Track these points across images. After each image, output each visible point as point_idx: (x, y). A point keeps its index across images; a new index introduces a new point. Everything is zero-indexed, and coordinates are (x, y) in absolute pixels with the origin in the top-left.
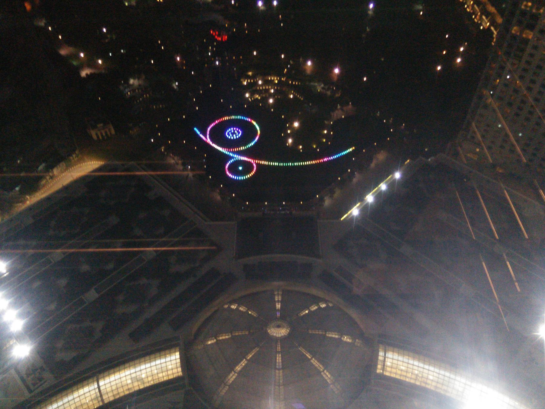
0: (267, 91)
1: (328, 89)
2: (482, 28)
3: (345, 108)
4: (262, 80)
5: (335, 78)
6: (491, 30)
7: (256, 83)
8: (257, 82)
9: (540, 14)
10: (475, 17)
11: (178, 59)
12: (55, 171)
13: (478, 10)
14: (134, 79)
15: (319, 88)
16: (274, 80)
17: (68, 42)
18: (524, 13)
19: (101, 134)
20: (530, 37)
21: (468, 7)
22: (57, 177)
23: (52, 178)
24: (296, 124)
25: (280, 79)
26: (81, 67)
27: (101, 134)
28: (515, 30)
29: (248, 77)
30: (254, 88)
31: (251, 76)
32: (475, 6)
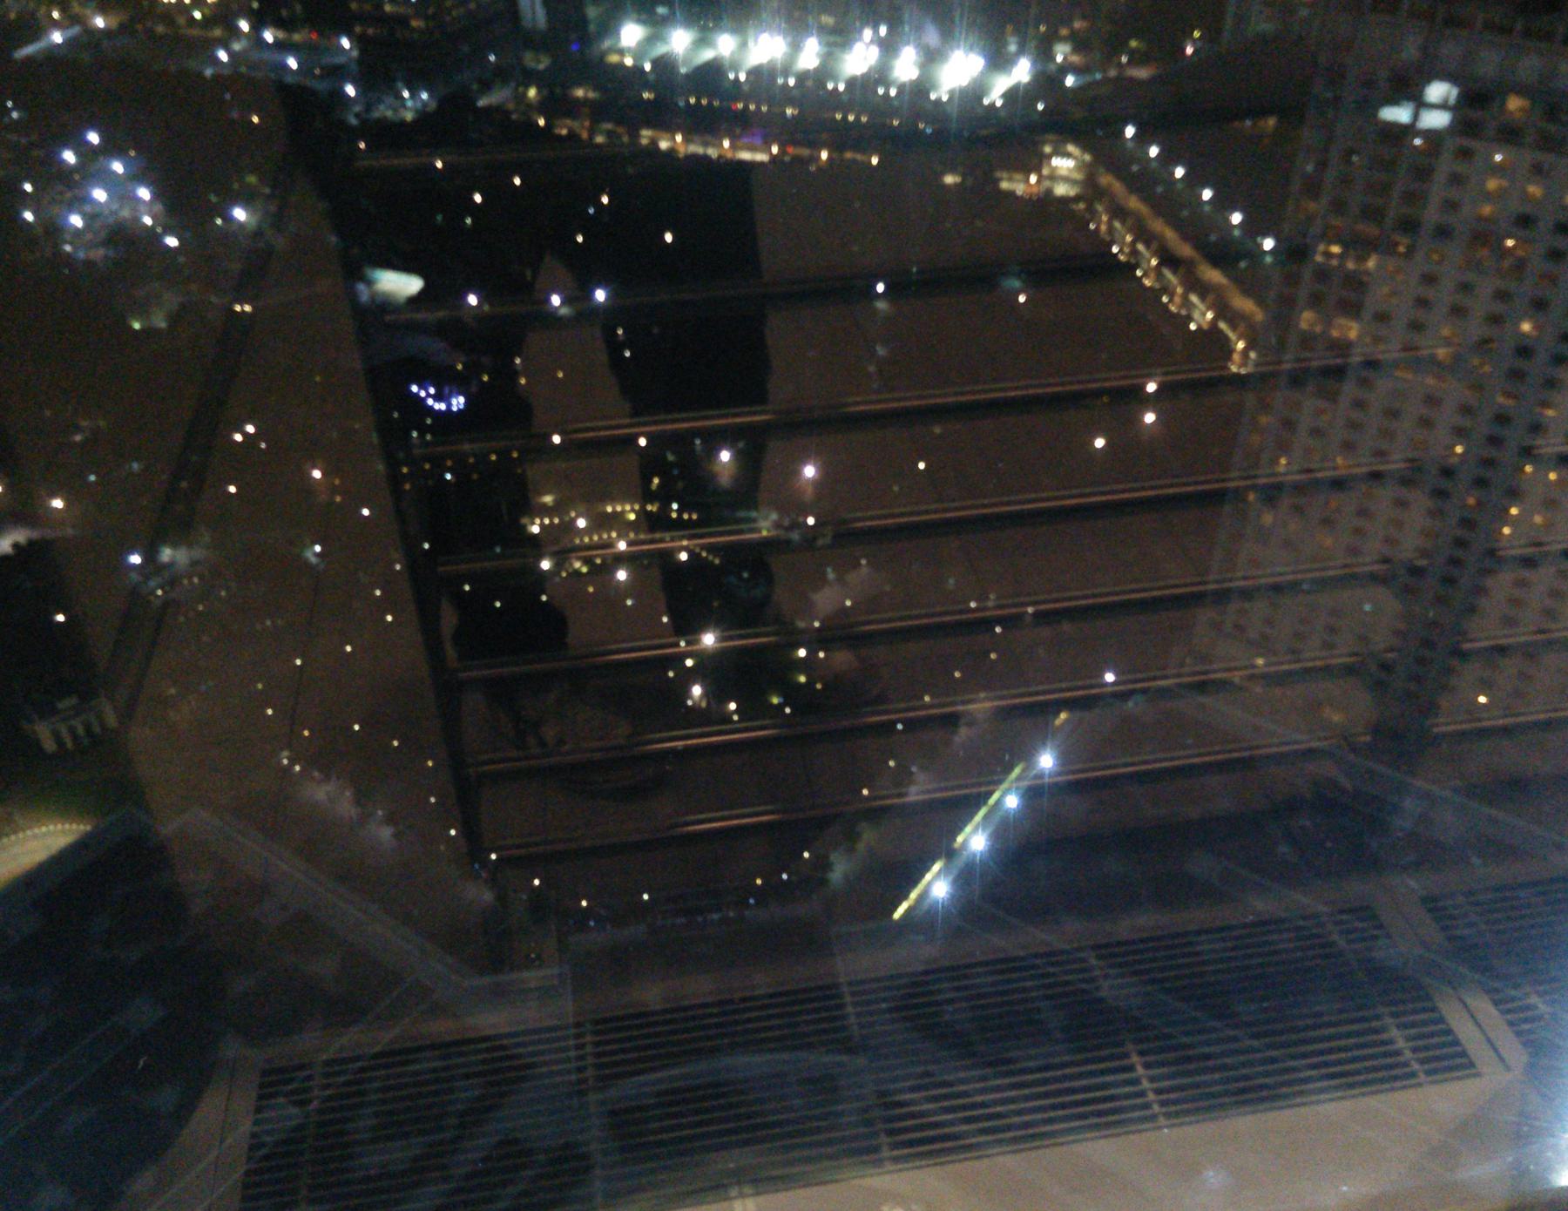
2: (1193, 327)
6: (1221, 332)
9: (1367, 273)
18: (1322, 274)
21: (1145, 274)
25: (643, 508)
28: (1307, 319)
31: (550, 507)
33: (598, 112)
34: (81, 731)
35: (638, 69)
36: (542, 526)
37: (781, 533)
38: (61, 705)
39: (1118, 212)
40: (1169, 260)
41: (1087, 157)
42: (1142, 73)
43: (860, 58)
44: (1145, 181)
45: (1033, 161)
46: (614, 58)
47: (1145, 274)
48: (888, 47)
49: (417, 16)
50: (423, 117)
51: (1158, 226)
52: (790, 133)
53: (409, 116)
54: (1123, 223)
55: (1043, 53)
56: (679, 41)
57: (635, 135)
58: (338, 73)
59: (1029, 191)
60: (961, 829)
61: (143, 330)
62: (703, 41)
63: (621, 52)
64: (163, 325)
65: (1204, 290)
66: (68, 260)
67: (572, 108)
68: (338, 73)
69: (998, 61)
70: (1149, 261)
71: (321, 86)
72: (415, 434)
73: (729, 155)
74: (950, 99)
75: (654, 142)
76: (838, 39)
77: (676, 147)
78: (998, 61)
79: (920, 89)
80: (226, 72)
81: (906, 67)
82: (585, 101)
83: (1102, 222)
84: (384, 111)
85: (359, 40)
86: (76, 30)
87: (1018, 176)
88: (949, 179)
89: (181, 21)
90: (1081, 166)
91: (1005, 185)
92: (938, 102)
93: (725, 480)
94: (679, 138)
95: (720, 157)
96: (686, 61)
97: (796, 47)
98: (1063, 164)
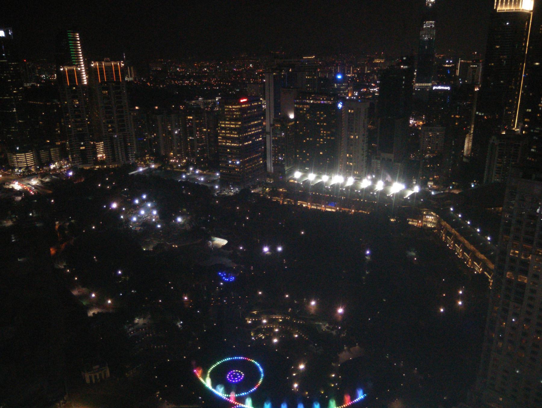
0: (271, 330)
1: (332, 330)
3: (351, 349)
4: (267, 319)
5: (340, 318)
6: (485, 274)
7: (260, 322)
10: (468, 263)
13: (469, 258)
14: (139, 318)
15: (324, 327)
17: (83, 283)
18: (513, 260)
19: (96, 376)
20: (526, 281)
24: (302, 367)
26: (89, 307)
27: (96, 376)
28: (508, 275)
29: (253, 316)
30: (259, 327)
32: (465, 253)
33: (286, 196)
34: (98, 377)
35: (298, 185)
38: (94, 367)
39: (448, 234)
40: (465, 249)
41: (438, 216)
42: (457, 192)
43: (365, 183)
44: (456, 225)
46: (292, 181)
47: (458, 254)
48: (374, 181)
49: (237, 168)
50: (236, 195)
51: (462, 239)
52: (343, 204)
53: (232, 194)
55: (423, 184)
56: (312, 177)
57: (296, 202)
58: (214, 182)
59: (418, 225)
62: (318, 177)
63: (295, 179)
65: (479, 261)
67: (278, 194)
68: (214, 182)
69: (409, 186)
71: (209, 185)
74: (393, 197)
75: (301, 205)
76: (359, 178)
77: (308, 206)
78: (409, 186)
79: (383, 193)
80: (183, 181)
81: (380, 186)
82: (282, 192)
84: (225, 193)
85: (221, 174)
86: (147, 168)
88: (392, 220)
89: (175, 167)
90: (436, 218)
91: (410, 223)
92: (389, 197)
94: (309, 204)
95: (321, 210)
96: (312, 182)
97: (346, 180)
98: (430, 218)
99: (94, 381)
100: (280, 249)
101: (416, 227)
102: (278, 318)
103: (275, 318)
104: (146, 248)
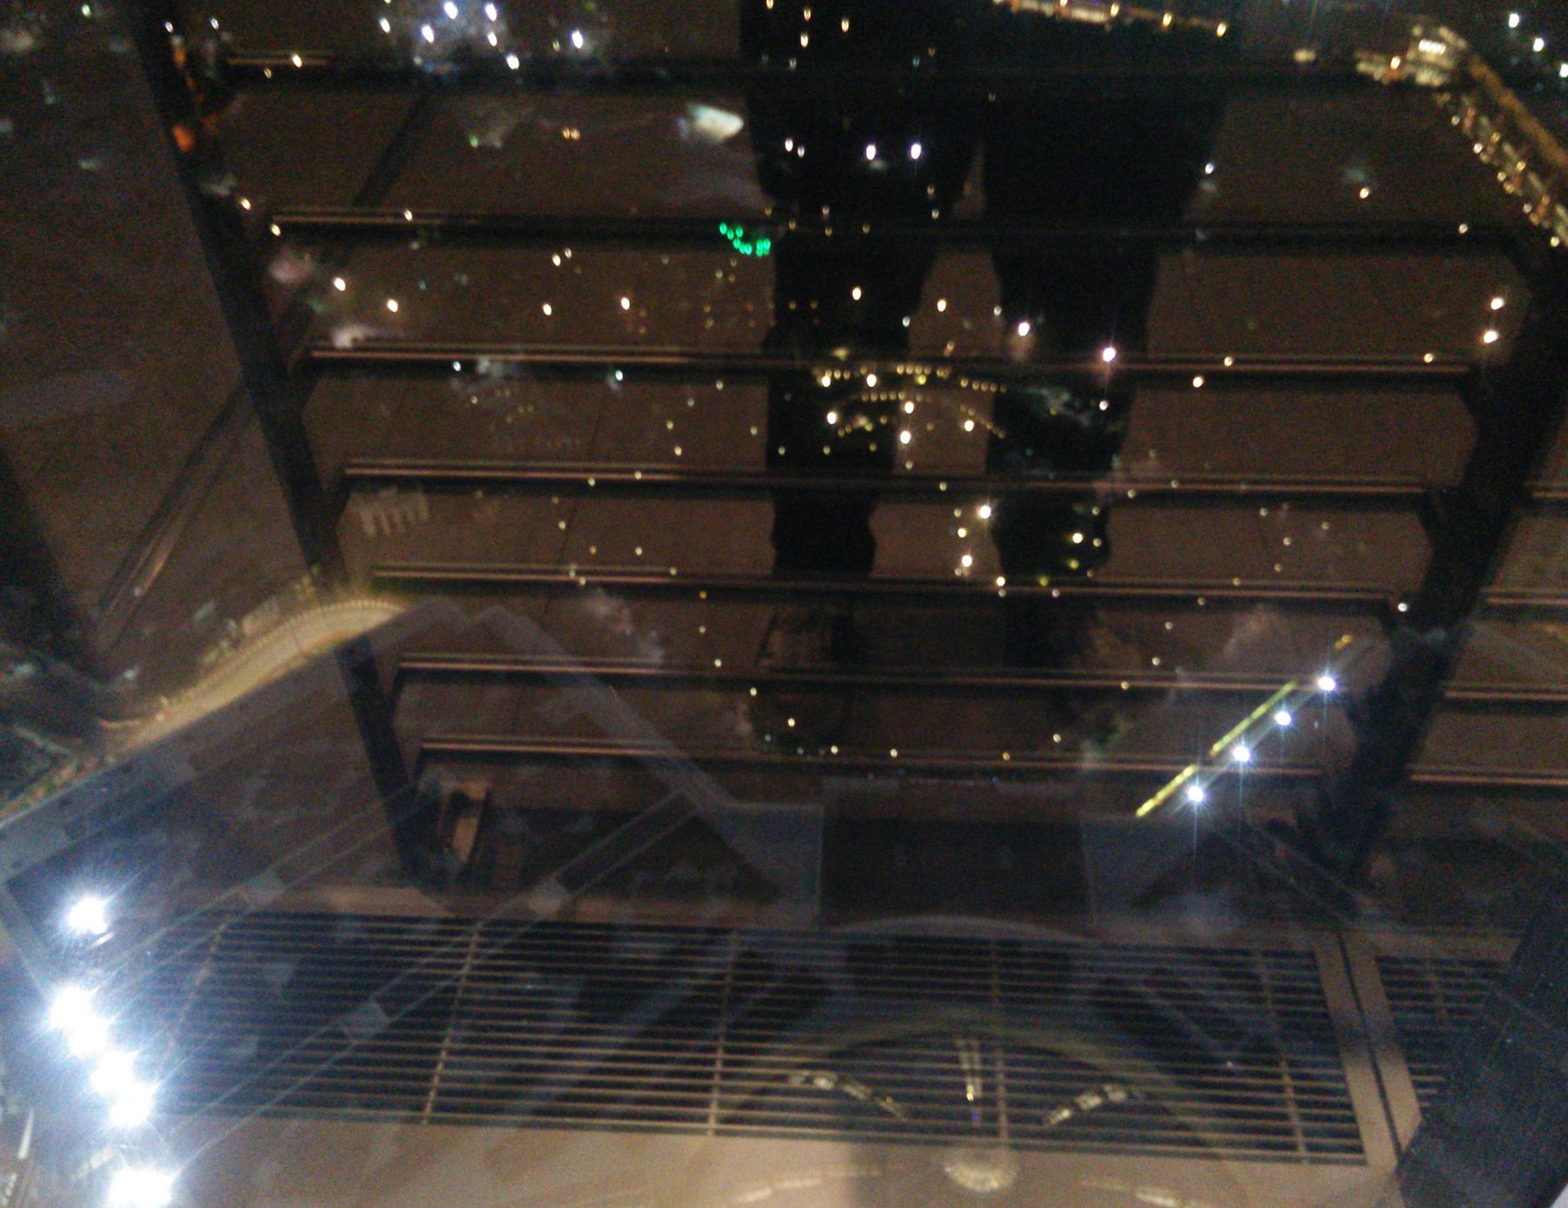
0: (893, 408)
1: (1081, 411)
2: (1554, 242)
8: (863, 379)
11: (625, 303)
12: (249, 625)
15: (1056, 403)
16: (913, 376)
21: (1508, 179)
22: (253, 639)
23: (236, 644)
27: (390, 517)
29: (834, 364)
30: (854, 397)
36: (833, 378)
37: (1070, 413)
39: (1488, 107)
41: (1462, 44)
45: (1400, 43)
51: (1531, 126)
54: (1491, 118)
60: (1218, 737)
61: (480, 148)
64: (498, 144)
66: (419, 72)
70: (1515, 165)
72: (719, 275)
73: (1065, 13)
83: (1464, 118)
87: (1377, 58)
90: (1452, 52)
91: (1362, 67)
93: (1019, 354)
98: (1431, 49)
99: (386, 528)
100: (916, 151)
101: (1379, 83)
102: (913, 376)
103: (905, 374)
104: (481, 136)
